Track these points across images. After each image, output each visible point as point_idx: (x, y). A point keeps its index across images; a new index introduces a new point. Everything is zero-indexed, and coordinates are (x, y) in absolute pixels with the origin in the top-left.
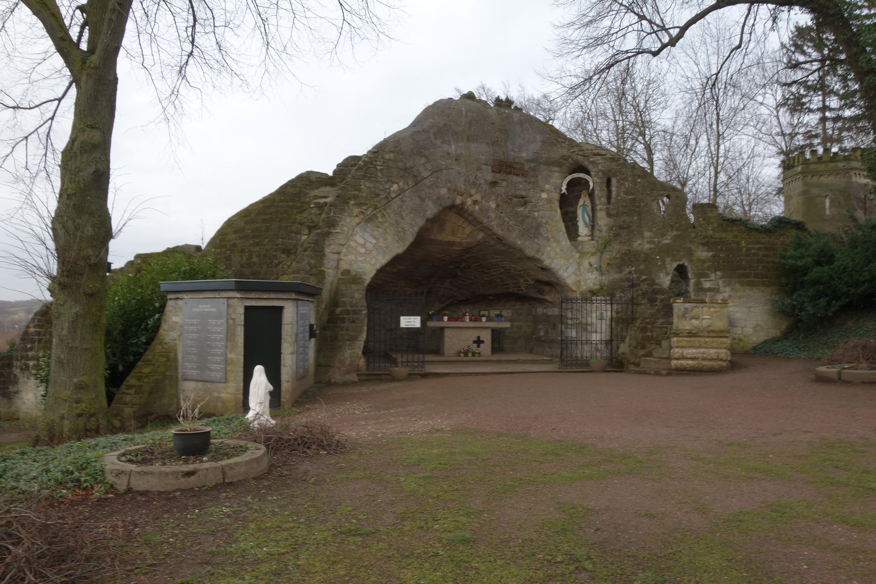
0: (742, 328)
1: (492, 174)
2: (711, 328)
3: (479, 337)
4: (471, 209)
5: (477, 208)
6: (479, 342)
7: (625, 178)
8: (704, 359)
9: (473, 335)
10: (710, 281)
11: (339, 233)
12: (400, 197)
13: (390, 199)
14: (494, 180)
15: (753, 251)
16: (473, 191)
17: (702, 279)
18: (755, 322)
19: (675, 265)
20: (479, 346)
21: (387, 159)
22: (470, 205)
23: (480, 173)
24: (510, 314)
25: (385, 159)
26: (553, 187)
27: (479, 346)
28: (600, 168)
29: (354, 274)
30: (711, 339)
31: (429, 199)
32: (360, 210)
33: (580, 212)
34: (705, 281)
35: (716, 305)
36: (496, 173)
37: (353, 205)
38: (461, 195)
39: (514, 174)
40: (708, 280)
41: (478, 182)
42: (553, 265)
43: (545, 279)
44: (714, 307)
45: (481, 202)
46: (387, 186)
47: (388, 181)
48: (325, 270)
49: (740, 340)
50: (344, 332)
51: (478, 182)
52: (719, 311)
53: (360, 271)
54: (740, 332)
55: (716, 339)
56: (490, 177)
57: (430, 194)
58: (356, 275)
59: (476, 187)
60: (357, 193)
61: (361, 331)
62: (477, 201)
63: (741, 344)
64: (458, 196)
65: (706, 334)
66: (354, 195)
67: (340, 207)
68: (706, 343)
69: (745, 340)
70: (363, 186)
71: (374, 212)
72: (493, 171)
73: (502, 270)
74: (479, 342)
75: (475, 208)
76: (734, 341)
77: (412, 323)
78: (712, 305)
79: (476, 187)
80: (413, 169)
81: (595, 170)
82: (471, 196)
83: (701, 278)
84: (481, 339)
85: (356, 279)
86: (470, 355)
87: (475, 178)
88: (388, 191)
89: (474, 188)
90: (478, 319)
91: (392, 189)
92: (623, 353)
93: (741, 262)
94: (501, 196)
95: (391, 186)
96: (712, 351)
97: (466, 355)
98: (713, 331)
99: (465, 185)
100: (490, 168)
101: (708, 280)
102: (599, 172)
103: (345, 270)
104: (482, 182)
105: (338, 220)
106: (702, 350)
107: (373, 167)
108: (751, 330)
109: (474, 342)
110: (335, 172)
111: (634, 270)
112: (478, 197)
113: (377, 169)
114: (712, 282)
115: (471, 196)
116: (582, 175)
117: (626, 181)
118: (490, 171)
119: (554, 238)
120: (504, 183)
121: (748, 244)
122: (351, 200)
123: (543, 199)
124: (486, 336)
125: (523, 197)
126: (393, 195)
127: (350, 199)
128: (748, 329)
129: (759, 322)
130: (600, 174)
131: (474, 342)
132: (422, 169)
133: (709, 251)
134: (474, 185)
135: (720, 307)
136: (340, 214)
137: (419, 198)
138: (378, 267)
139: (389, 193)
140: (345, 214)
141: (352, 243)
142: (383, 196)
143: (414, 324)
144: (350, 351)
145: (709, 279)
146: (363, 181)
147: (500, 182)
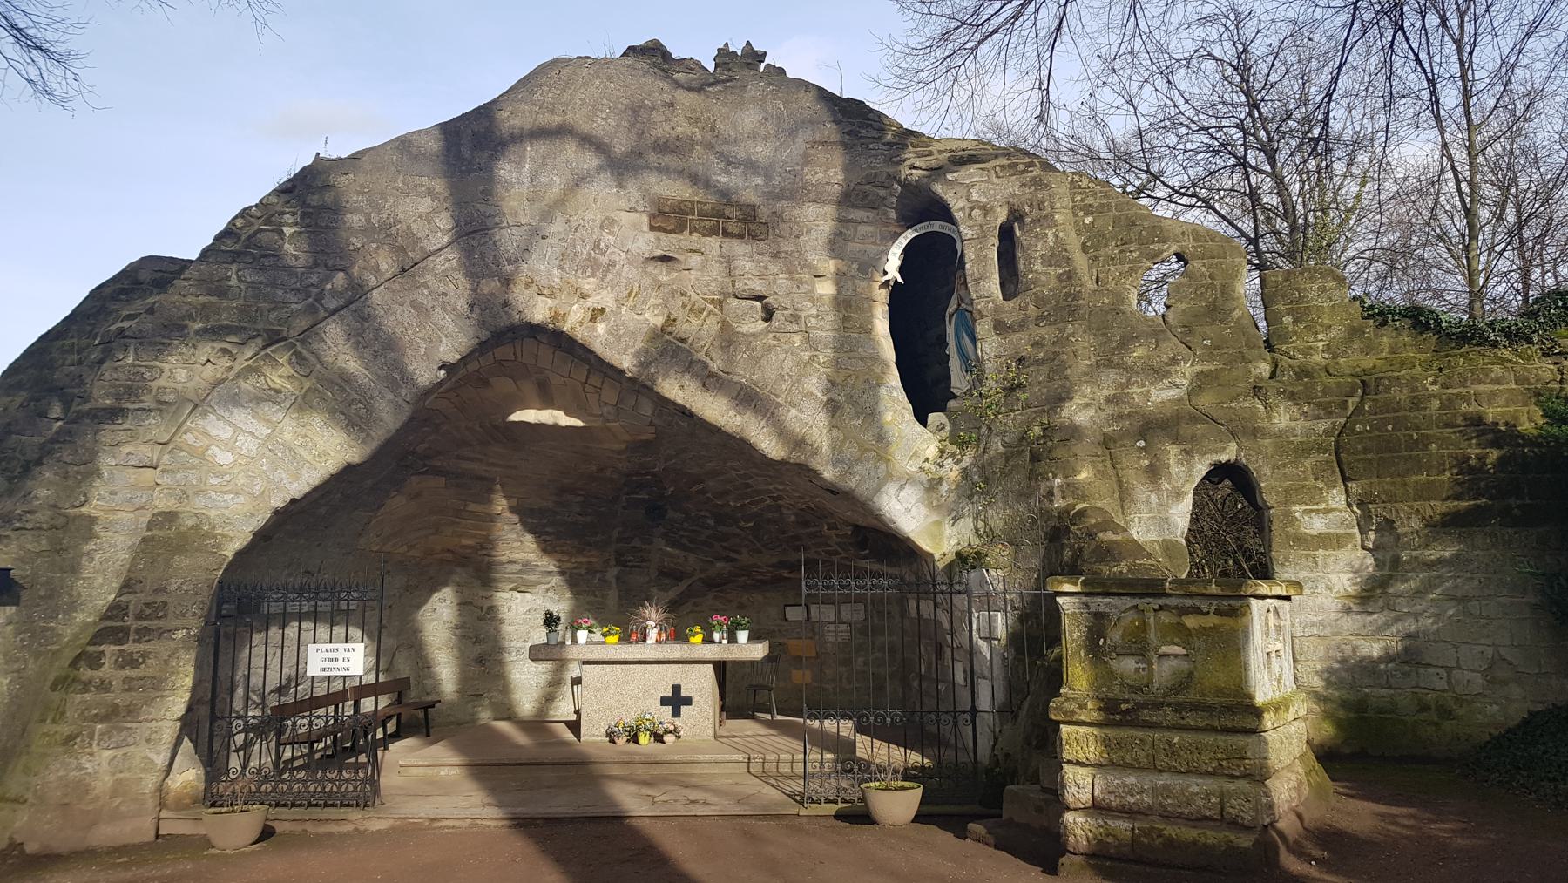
0: (1448, 669)
1: (651, 236)
2: (1192, 696)
3: (676, 689)
4: (580, 334)
5: (601, 328)
6: (676, 701)
7: (1046, 216)
8: (1167, 816)
9: (662, 680)
10: (1327, 511)
11: (150, 410)
12: (353, 307)
13: (322, 314)
14: (659, 252)
15: (1464, 407)
16: (588, 284)
17: (1298, 510)
18: (1490, 651)
19: (1202, 468)
20: (676, 713)
21: (314, 207)
22: (581, 323)
23: (609, 233)
24: (861, 616)
25: (309, 206)
26: (855, 266)
27: (676, 713)
28: (975, 196)
29: (190, 523)
30: (1189, 737)
31: (444, 309)
32: (218, 345)
33: (950, 331)
34: (1305, 512)
35: (1203, 604)
36: (665, 231)
37: (197, 333)
38: (551, 296)
39: (726, 234)
40: (1318, 512)
41: (604, 260)
42: (852, 482)
43: (861, 522)
44: (1197, 611)
45: (617, 313)
46: (314, 279)
47: (316, 264)
48: (94, 513)
49: (1445, 713)
50: (87, 696)
51: (604, 260)
52: (1215, 628)
53: (212, 513)
54: (1441, 684)
55: (1208, 739)
56: (646, 242)
57: (445, 294)
58: (196, 527)
59: (599, 274)
60: (214, 299)
61: (156, 687)
62: (603, 309)
63: (1447, 726)
64: (541, 298)
65: (1170, 716)
66: (204, 305)
67: (158, 339)
68: (1172, 751)
69: (1461, 712)
70: (234, 281)
71: (268, 350)
72: (652, 228)
73: (769, 502)
74: (676, 701)
75: (594, 329)
76: (1422, 716)
77: (340, 664)
78: (1188, 602)
79: (599, 274)
80: (393, 230)
81: (961, 204)
82: (584, 296)
83: (1294, 503)
84: (684, 693)
85: (195, 539)
86: (644, 739)
87: (596, 246)
88: (314, 291)
89: (593, 275)
90: (680, 637)
91: (329, 286)
92: (1007, 755)
93: (1426, 447)
94: (683, 294)
95: (328, 279)
96: (1196, 786)
97: (634, 739)
98: (1196, 707)
99: (562, 269)
100: (645, 218)
101: (1318, 512)
102: (972, 209)
103: (159, 514)
104: (620, 257)
105: (147, 375)
106: (1163, 780)
107: (272, 231)
108: (1479, 680)
109: (664, 701)
110: (205, 253)
111: (1060, 486)
112: (605, 299)
113: (281, 233)
114: (1330, 516)
115: (584, 296)
116: (936, 226)
117: (1050, 227)
118: (646, 228)
119: (851, 400)
120: (695, 260)
121: (1444, 386)
122: (195, 321)
123: (820, 298)
124: (701, 685)
125: (759, 298)
126: (333, 304)
127: (191, 317)
128: (1468, 675)
129: (1503, 652)
130: (976, 213)
131: (664, 701)
132: (420, 228)
133: (1318, 418)
134: (592, 266)
135: (1218, 612)
136: (156, 360)
137: (415, 308)
138: (278, 502)
139: (319, 298)
140: (172, 359)
141: (189, 438)
142: (299, 306)
143: (345, 664)
144: (108, 754)
145: (1322, 506)
146: (234, 267)
147: (681, 258)
